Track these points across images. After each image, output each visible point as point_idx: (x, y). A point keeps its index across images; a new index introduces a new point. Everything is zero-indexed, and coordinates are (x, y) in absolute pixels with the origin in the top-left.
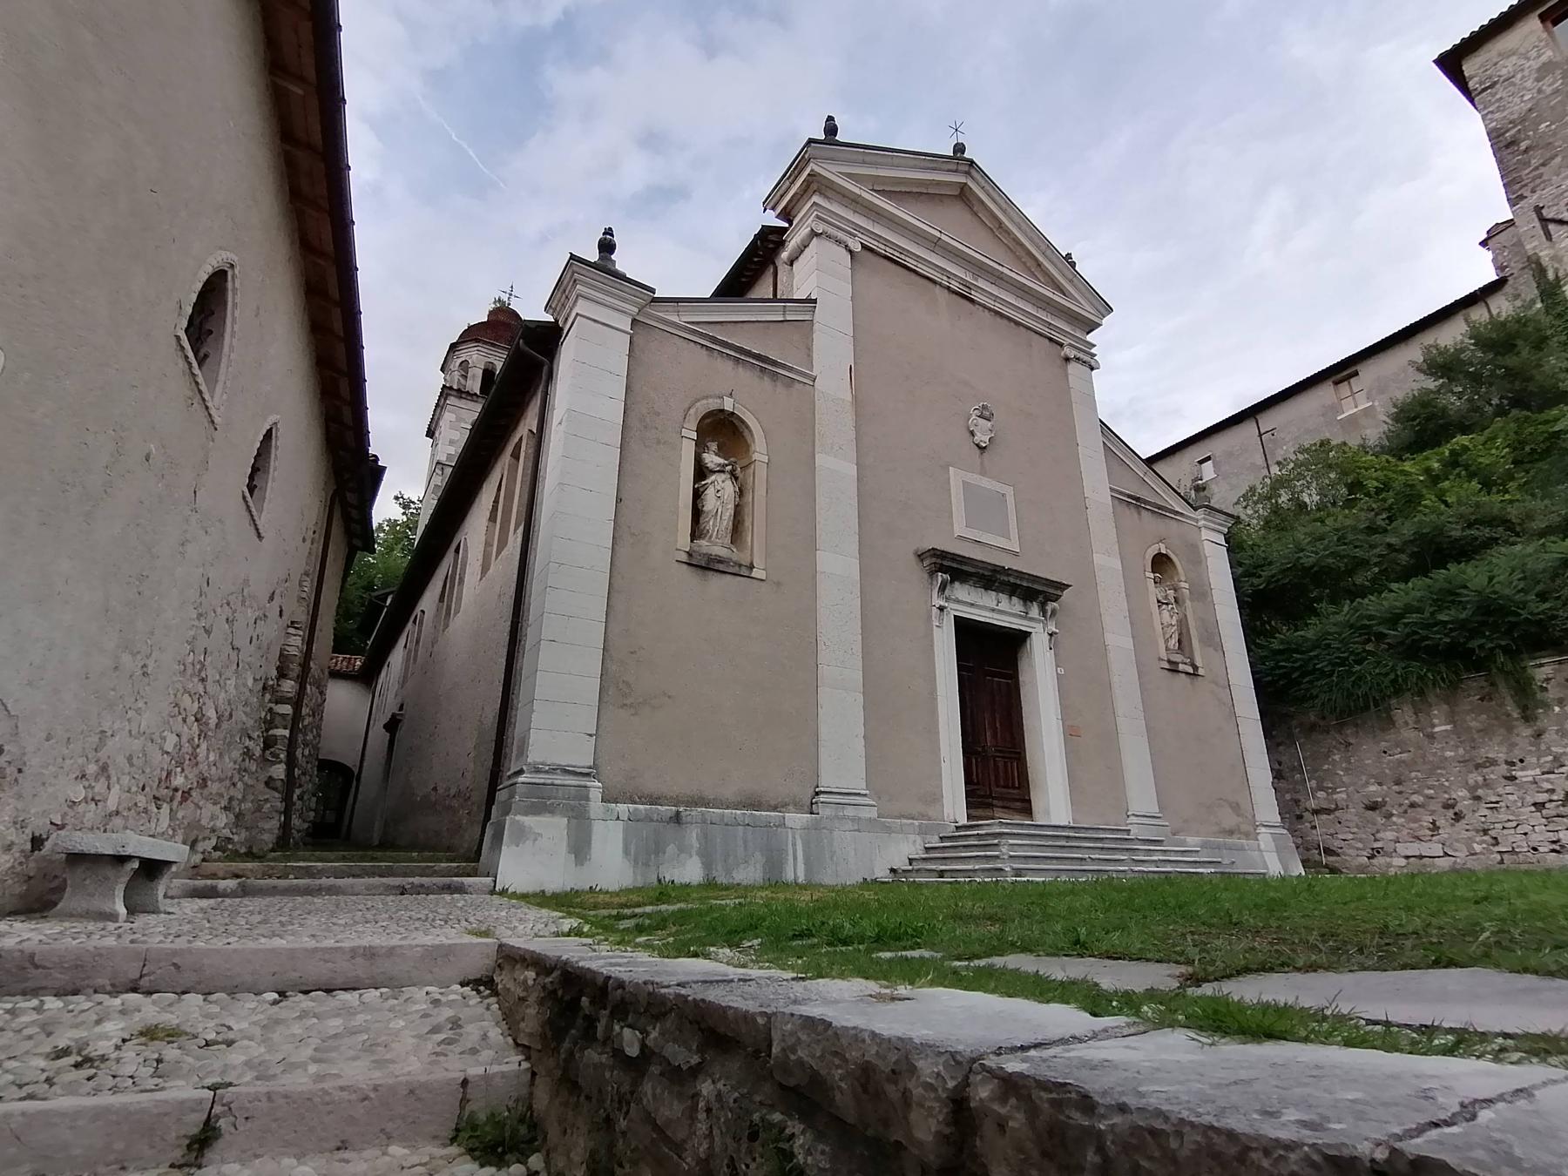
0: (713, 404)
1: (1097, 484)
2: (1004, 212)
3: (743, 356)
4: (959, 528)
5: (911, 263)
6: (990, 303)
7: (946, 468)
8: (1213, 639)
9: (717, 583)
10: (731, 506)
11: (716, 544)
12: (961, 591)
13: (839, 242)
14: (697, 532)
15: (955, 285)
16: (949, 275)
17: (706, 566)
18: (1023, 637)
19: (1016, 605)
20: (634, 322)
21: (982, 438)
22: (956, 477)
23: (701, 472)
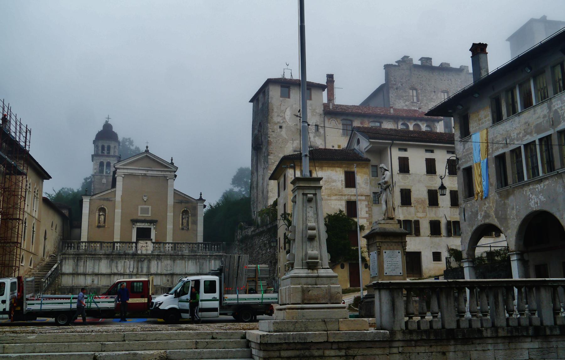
0: (100, 207)
1: (171, 200)
2: (154, 157)
3: (104, 200)
4: (139, 215)
5: (134, 174)
6: (150, 175)
7: (138, 206)
8: (195, 223)
9: (101, 229)
10: (103, 219)
11: (102, 224)
12: (138, 224)
13: (120, 176)
14: (99, 222)
15: (143, 175)
16: (141, 174)
17: (99, 227)
18: (150, 228)
19: (149, 224)
20: (90, 199)
21: (145, 200)
22: (140, 207)
23: (99, 215)
